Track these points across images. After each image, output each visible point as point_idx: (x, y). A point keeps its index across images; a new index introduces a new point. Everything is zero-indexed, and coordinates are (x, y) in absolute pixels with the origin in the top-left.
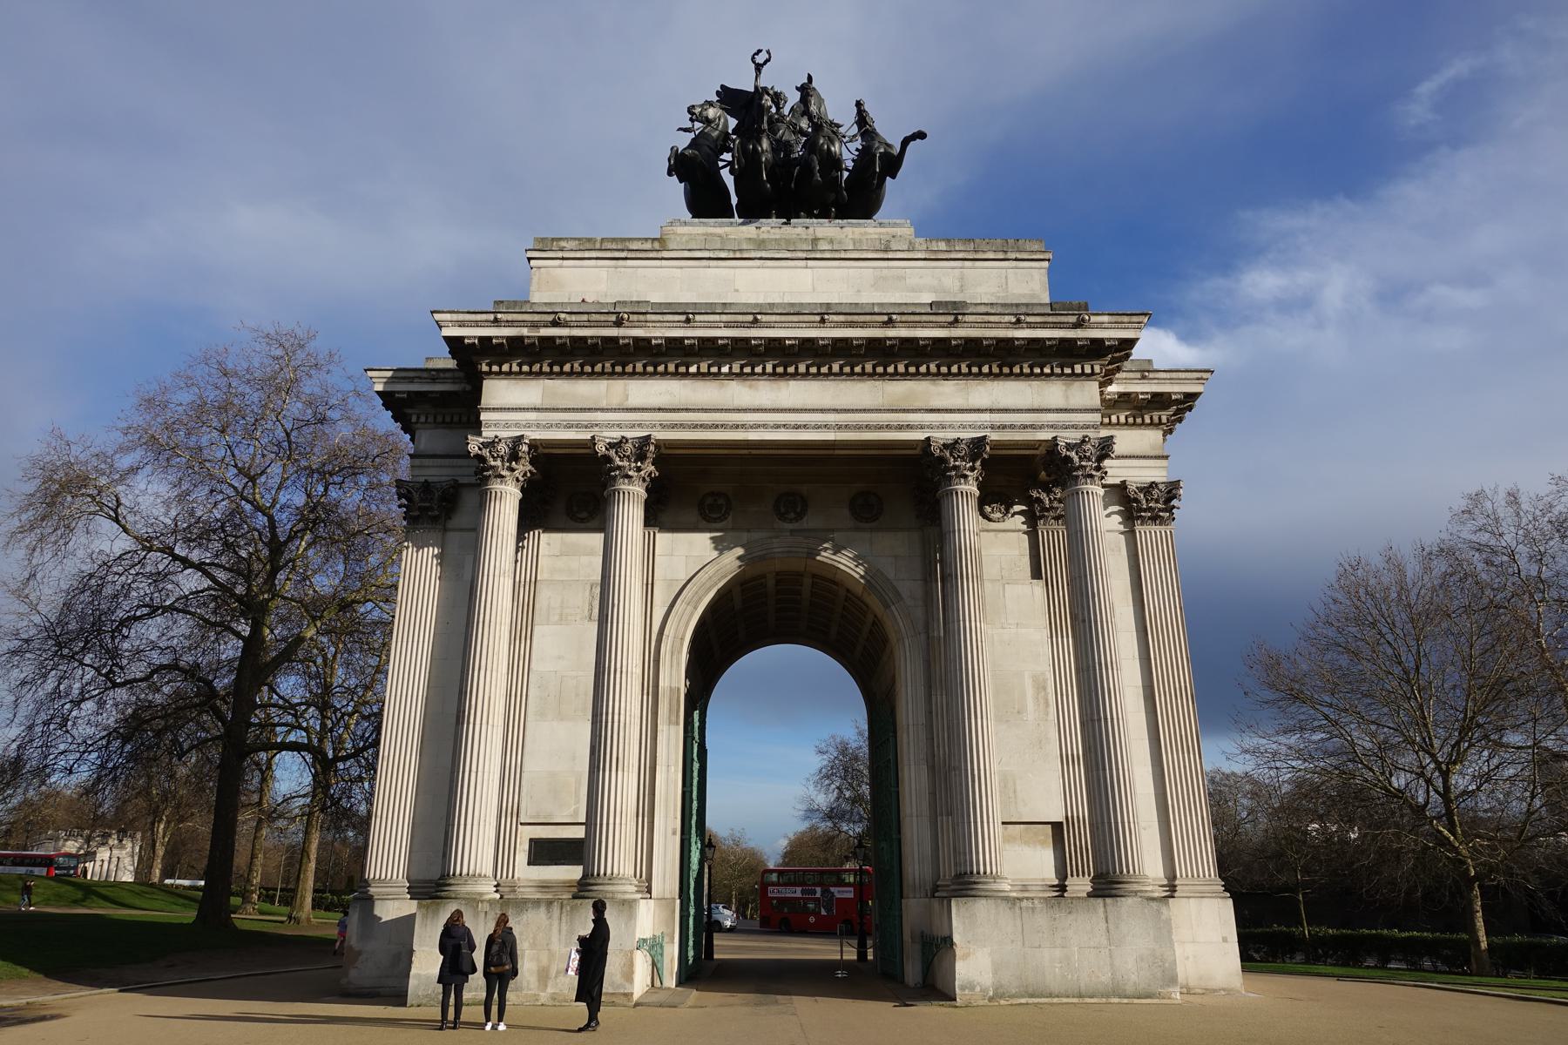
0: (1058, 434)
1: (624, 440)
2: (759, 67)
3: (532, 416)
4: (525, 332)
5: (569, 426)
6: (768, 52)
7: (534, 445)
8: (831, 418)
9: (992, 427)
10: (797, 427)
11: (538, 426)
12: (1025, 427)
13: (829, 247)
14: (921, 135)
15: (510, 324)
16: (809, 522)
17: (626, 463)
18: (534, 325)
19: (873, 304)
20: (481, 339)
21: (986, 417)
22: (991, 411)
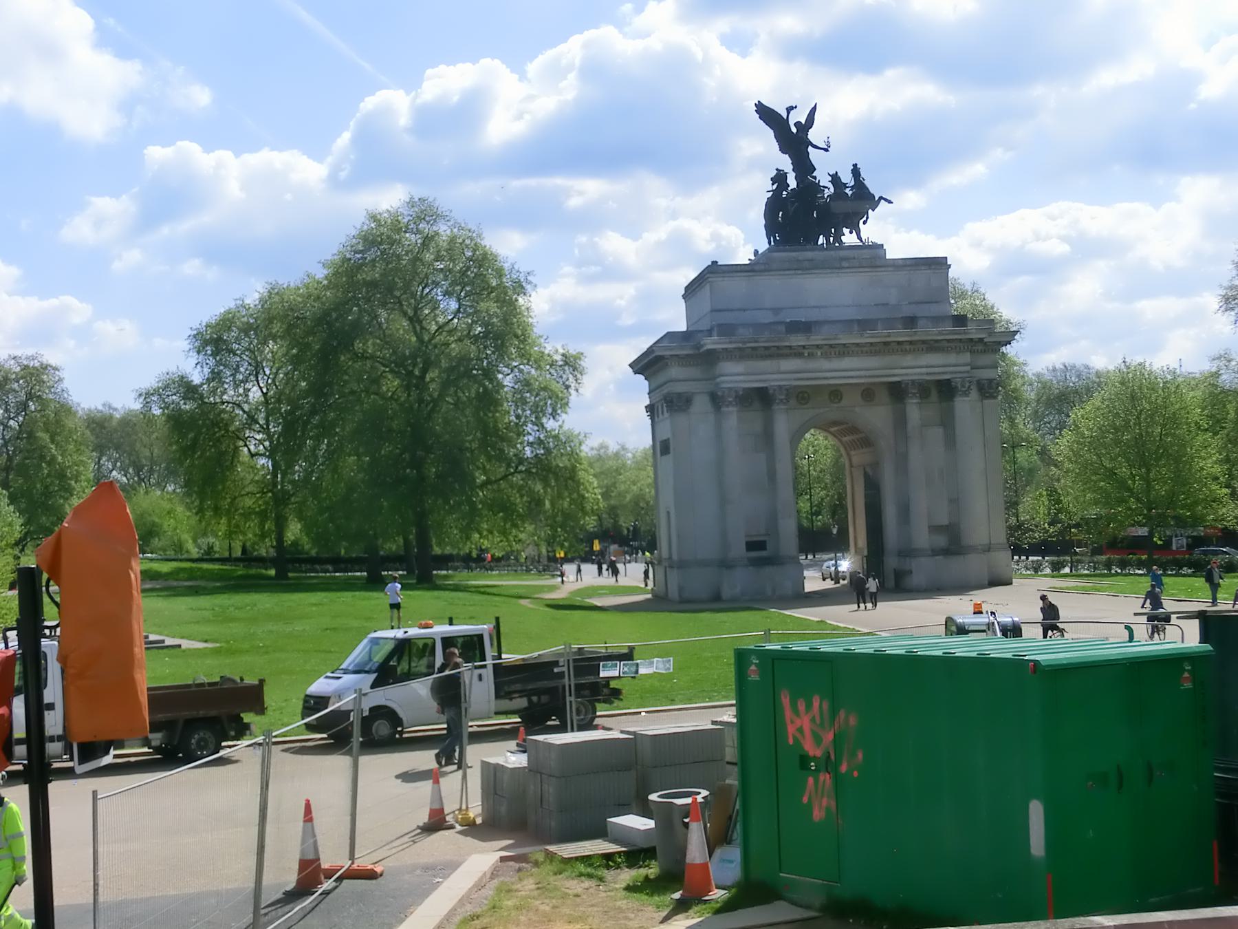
0: (954, 376)
1: (780, 387)
2: (788, 113)
3: (741, 378)
4: (741, 345)
5: (757, 381)
6: (796, 107)
7: (744, 389)
8: (862, 373)
9: (927, 374)
10: (849, 377)
11: (745, 381)
12: (939, 373)
13: (847, 265)
14: (890, 202)
15: (735, 342)
16: (844, 402)
17: (783, 397)
18: (744, 343)
19: (878, 319)
20: (723, 349)
21: (924, 370)
22: (927, 367)
